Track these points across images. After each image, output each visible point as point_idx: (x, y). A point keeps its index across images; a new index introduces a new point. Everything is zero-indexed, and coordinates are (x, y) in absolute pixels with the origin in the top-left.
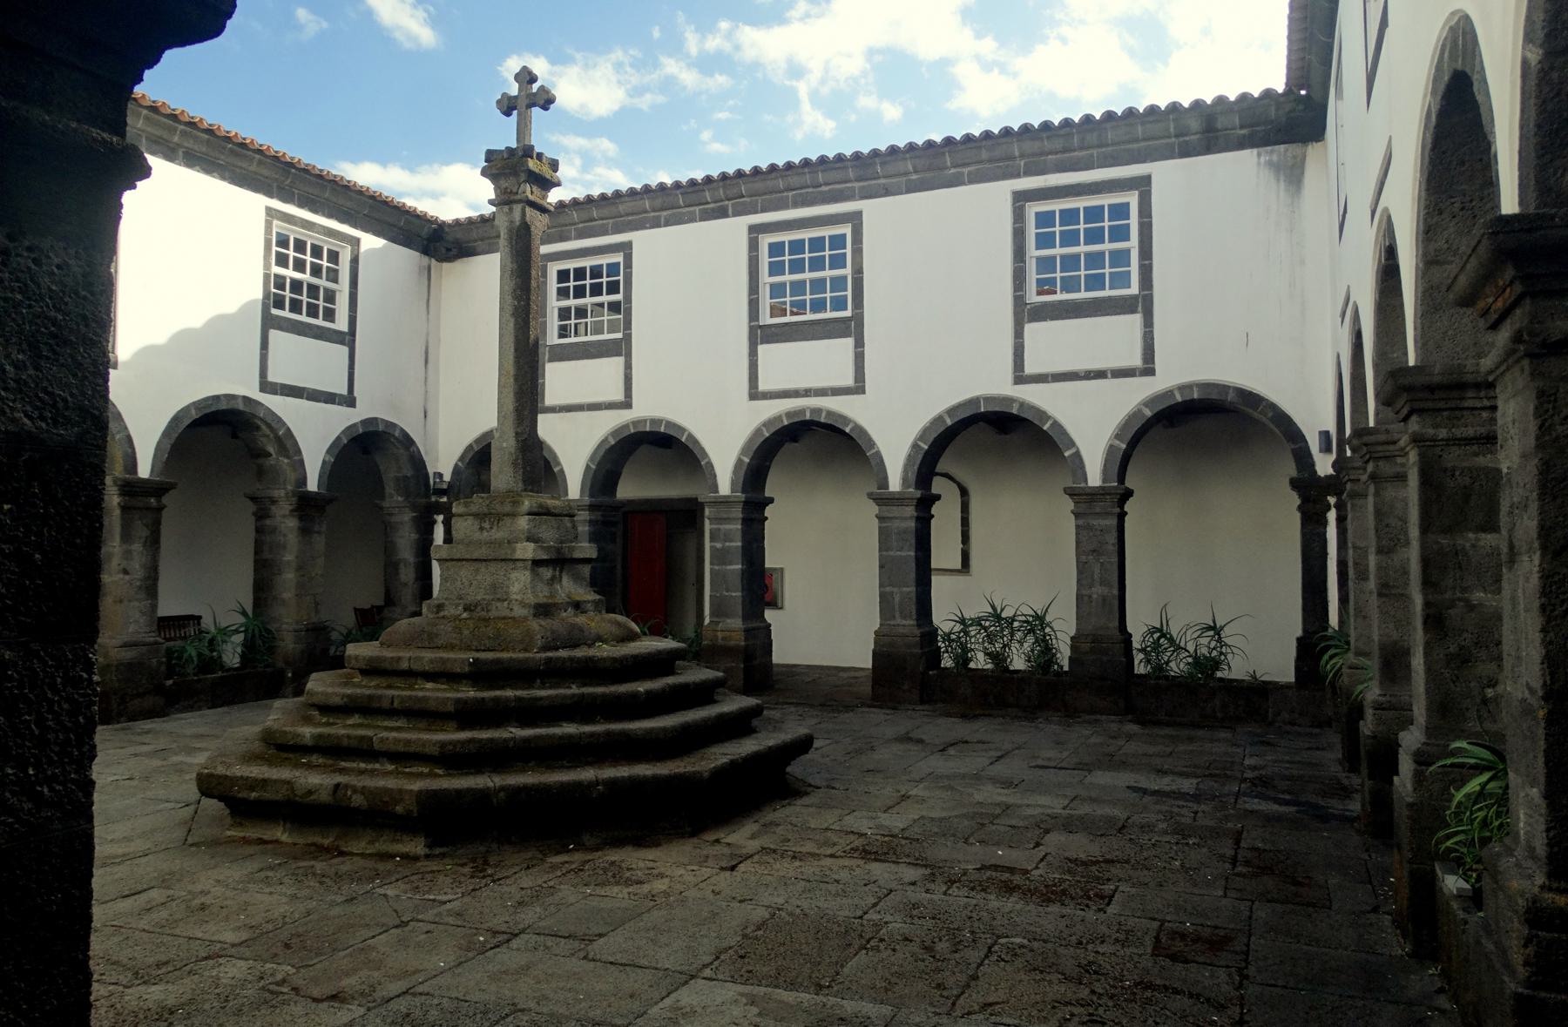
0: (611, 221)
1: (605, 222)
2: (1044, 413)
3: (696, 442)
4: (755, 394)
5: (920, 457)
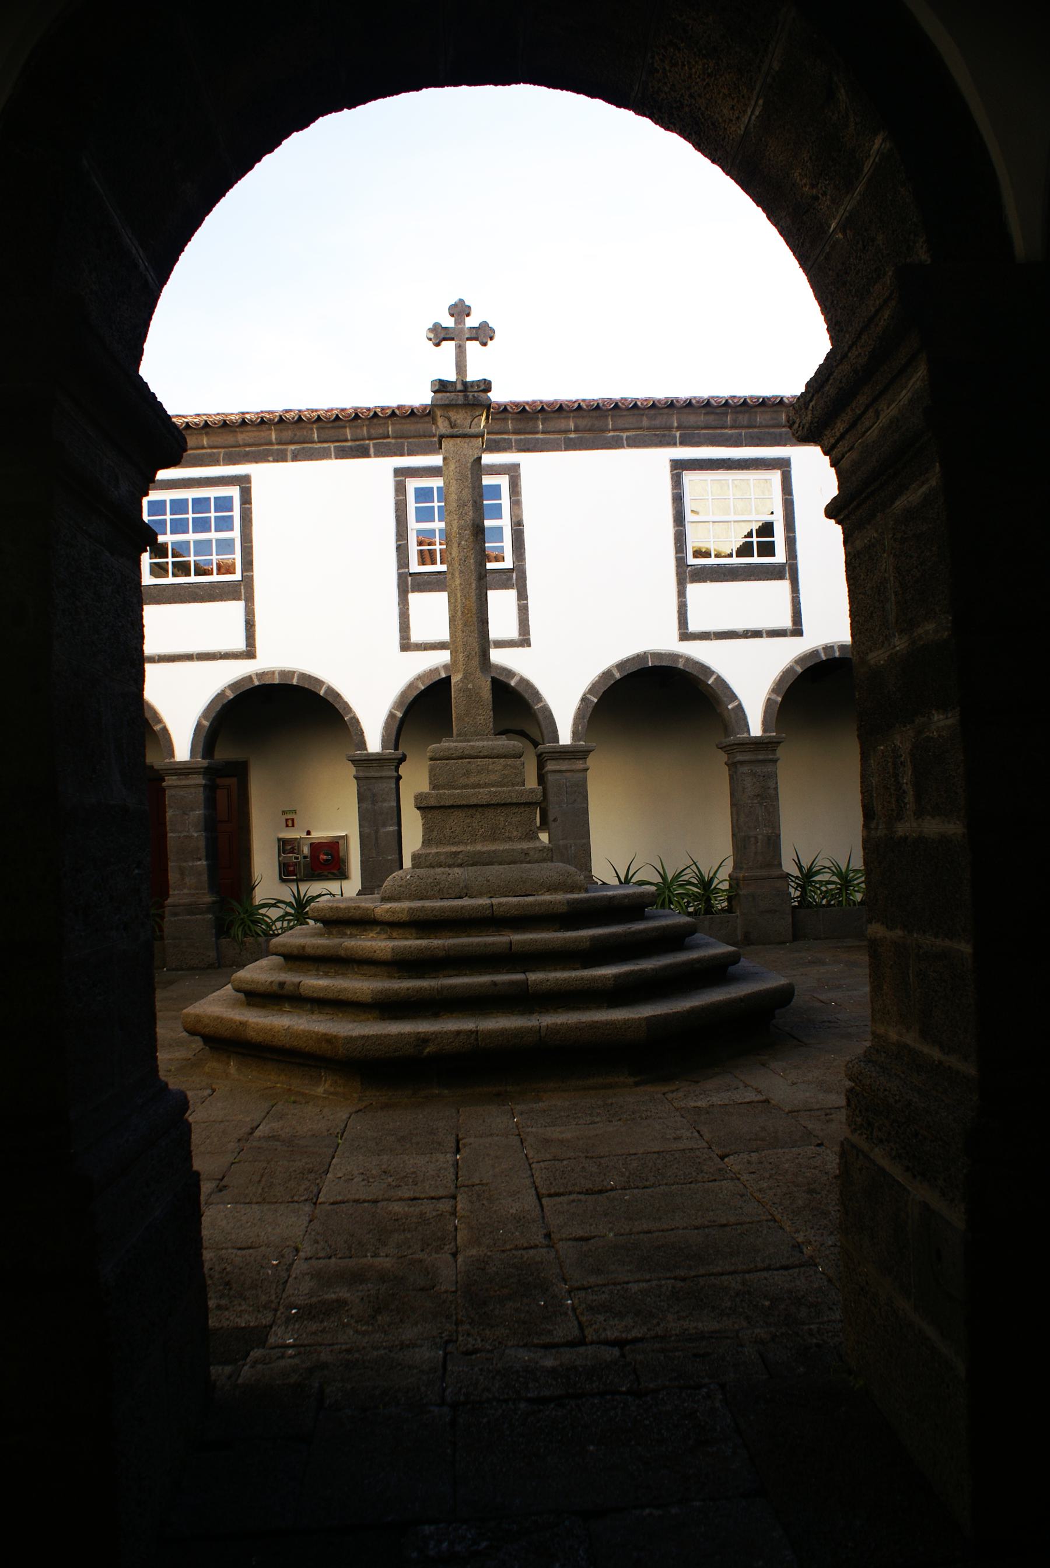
0: (222, 451)
1: (215, 451)
2: (708, 668)
3: (338, 696)
4: (406, 646)
5: (590, 710)
